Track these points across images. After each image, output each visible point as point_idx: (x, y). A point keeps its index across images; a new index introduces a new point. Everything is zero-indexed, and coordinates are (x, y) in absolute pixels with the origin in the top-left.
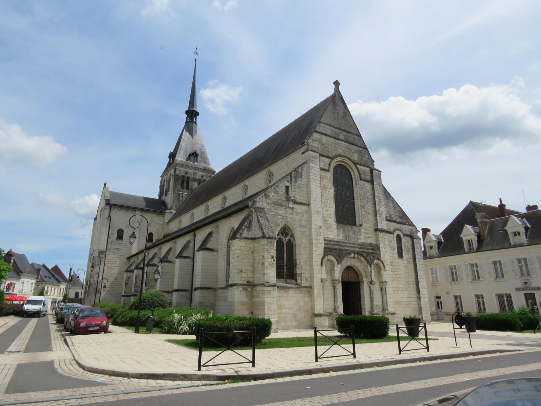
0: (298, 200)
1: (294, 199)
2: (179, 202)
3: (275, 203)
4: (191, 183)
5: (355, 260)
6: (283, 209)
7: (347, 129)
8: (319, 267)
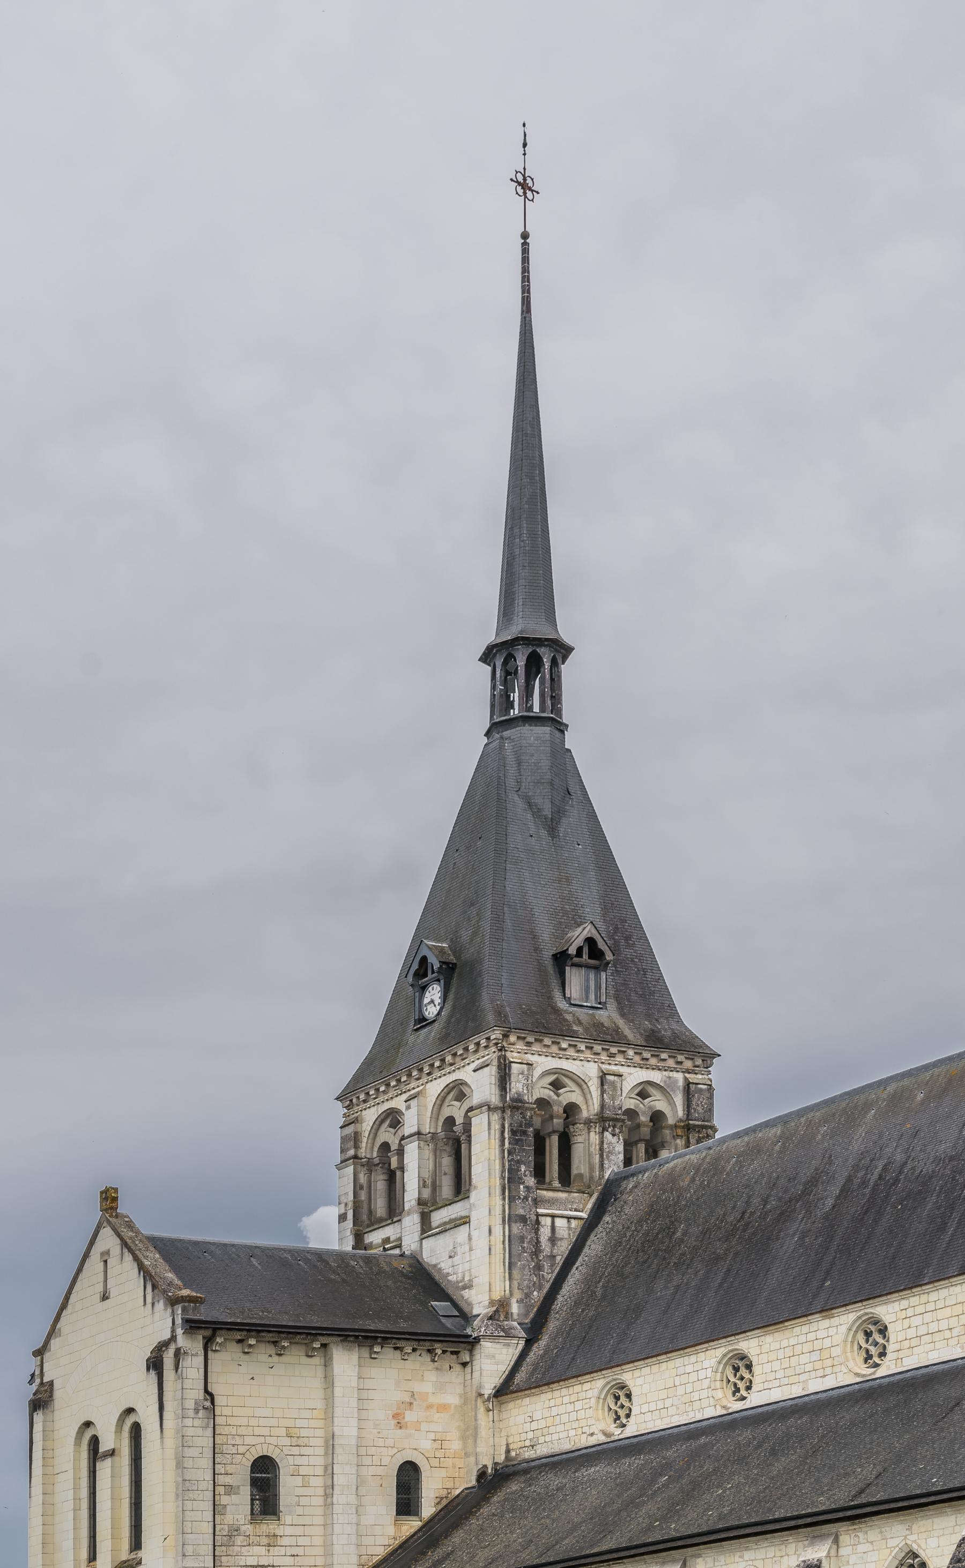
2: (539, 1267)
4: (586, 1143)
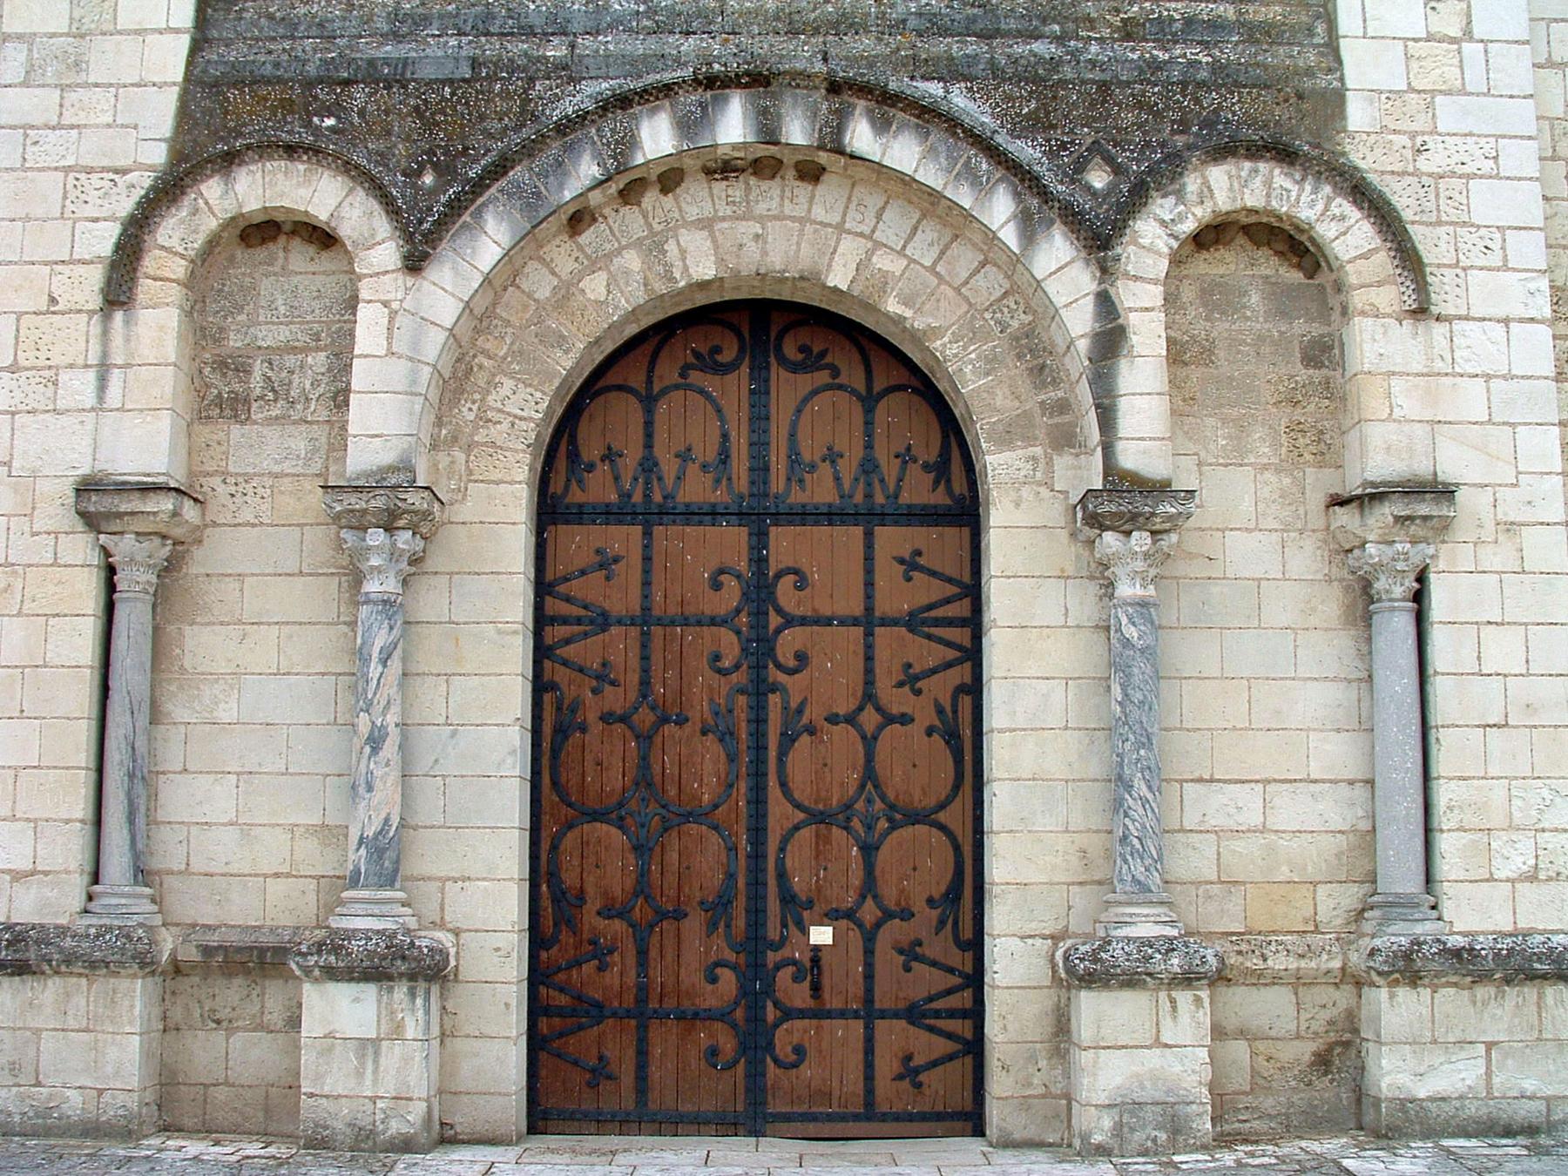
5: (825, 202)
8: (75, 337)
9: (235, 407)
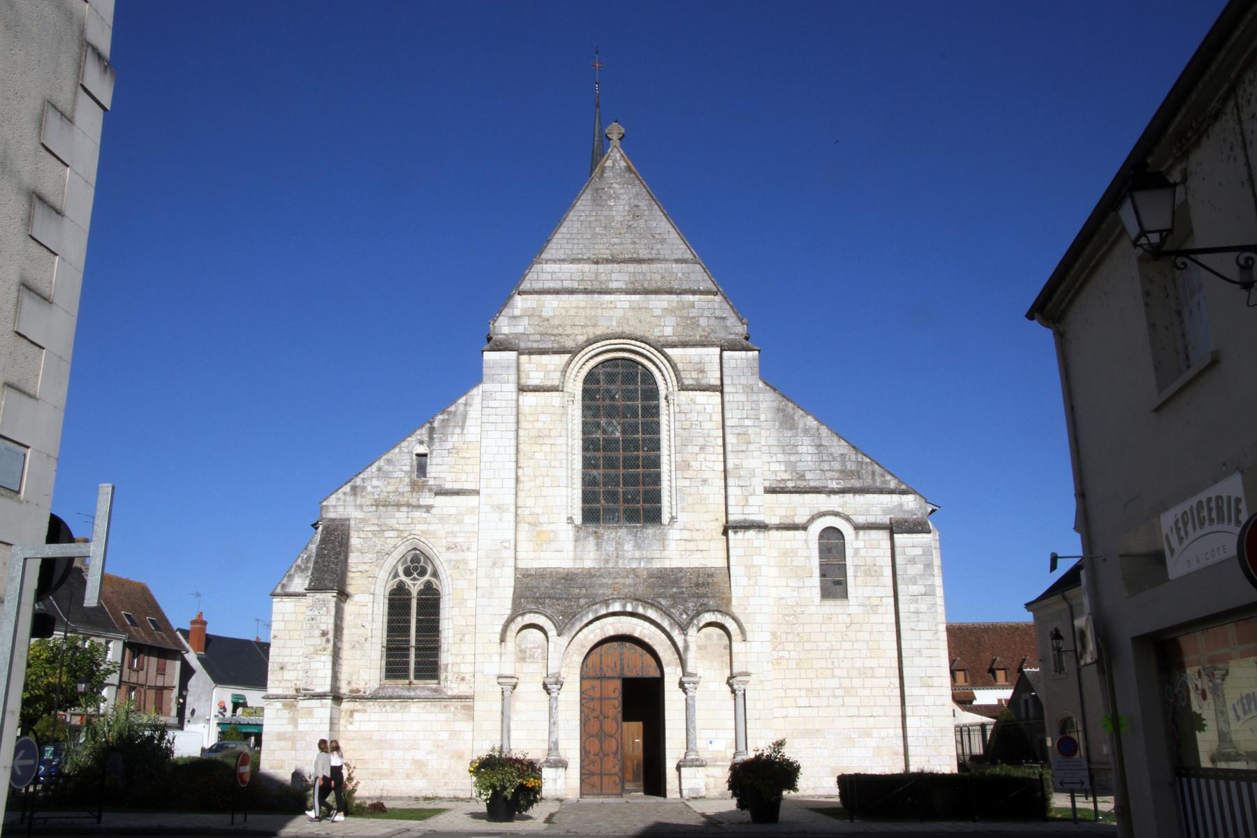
0: (448, 486)
1: (438, 482)
3: (377, 504)
6: (402, 514)
7: (643, 254)
8: (495, 647)
9: (523, 659)
